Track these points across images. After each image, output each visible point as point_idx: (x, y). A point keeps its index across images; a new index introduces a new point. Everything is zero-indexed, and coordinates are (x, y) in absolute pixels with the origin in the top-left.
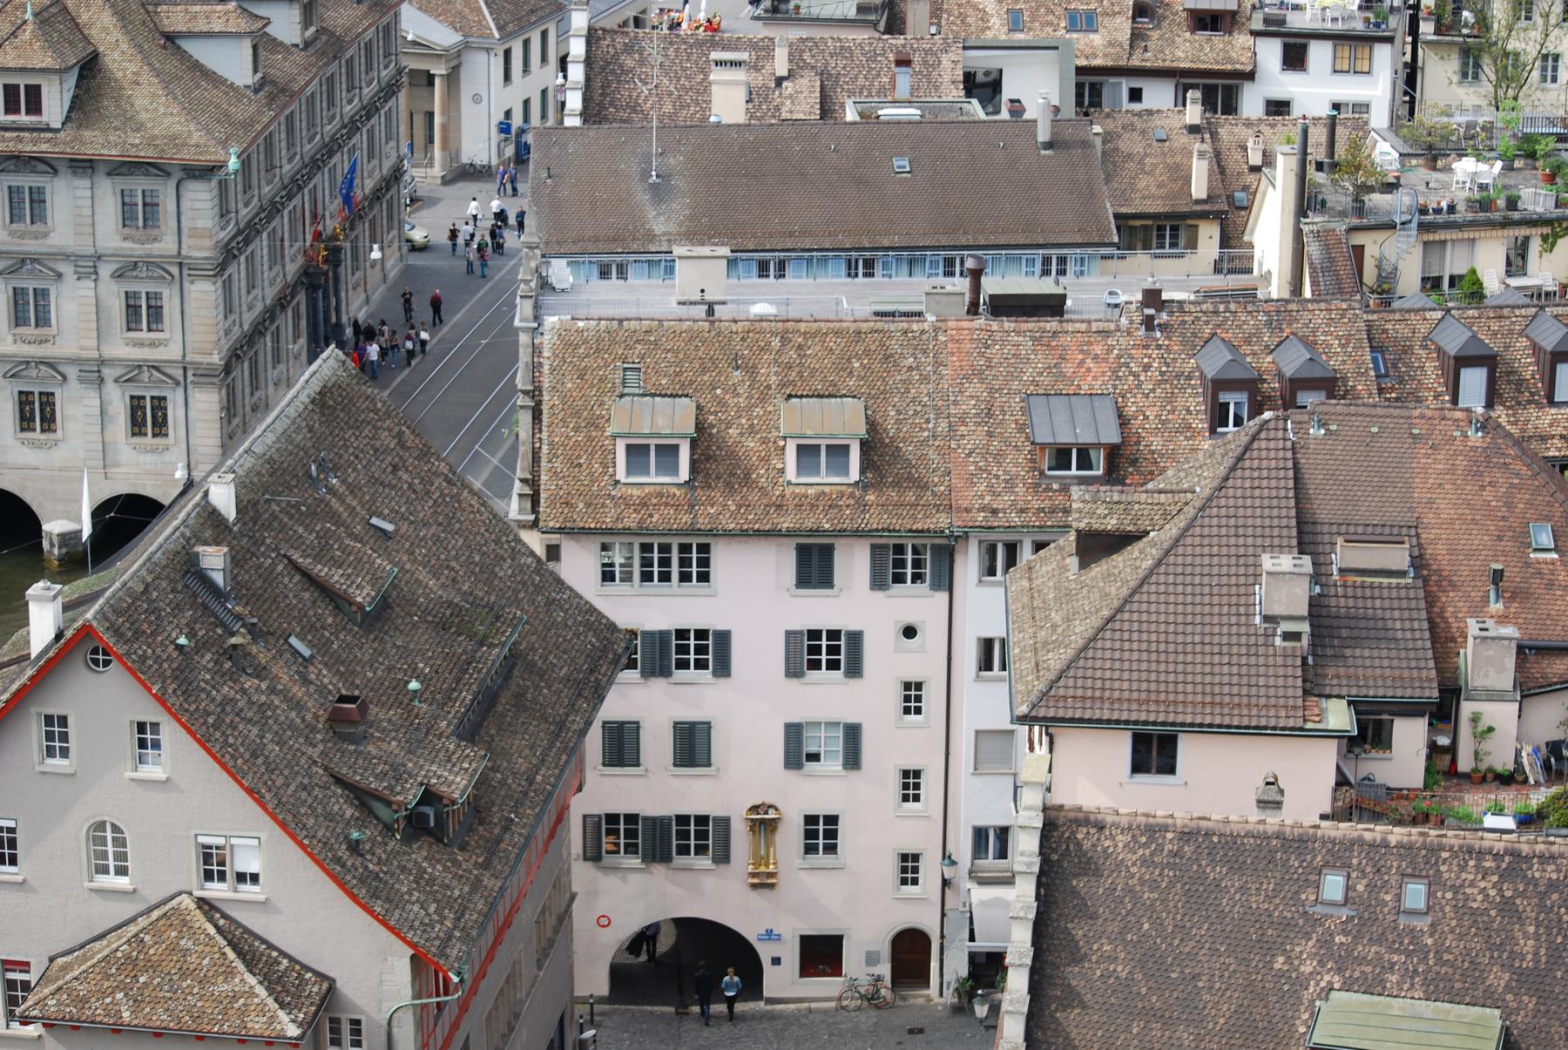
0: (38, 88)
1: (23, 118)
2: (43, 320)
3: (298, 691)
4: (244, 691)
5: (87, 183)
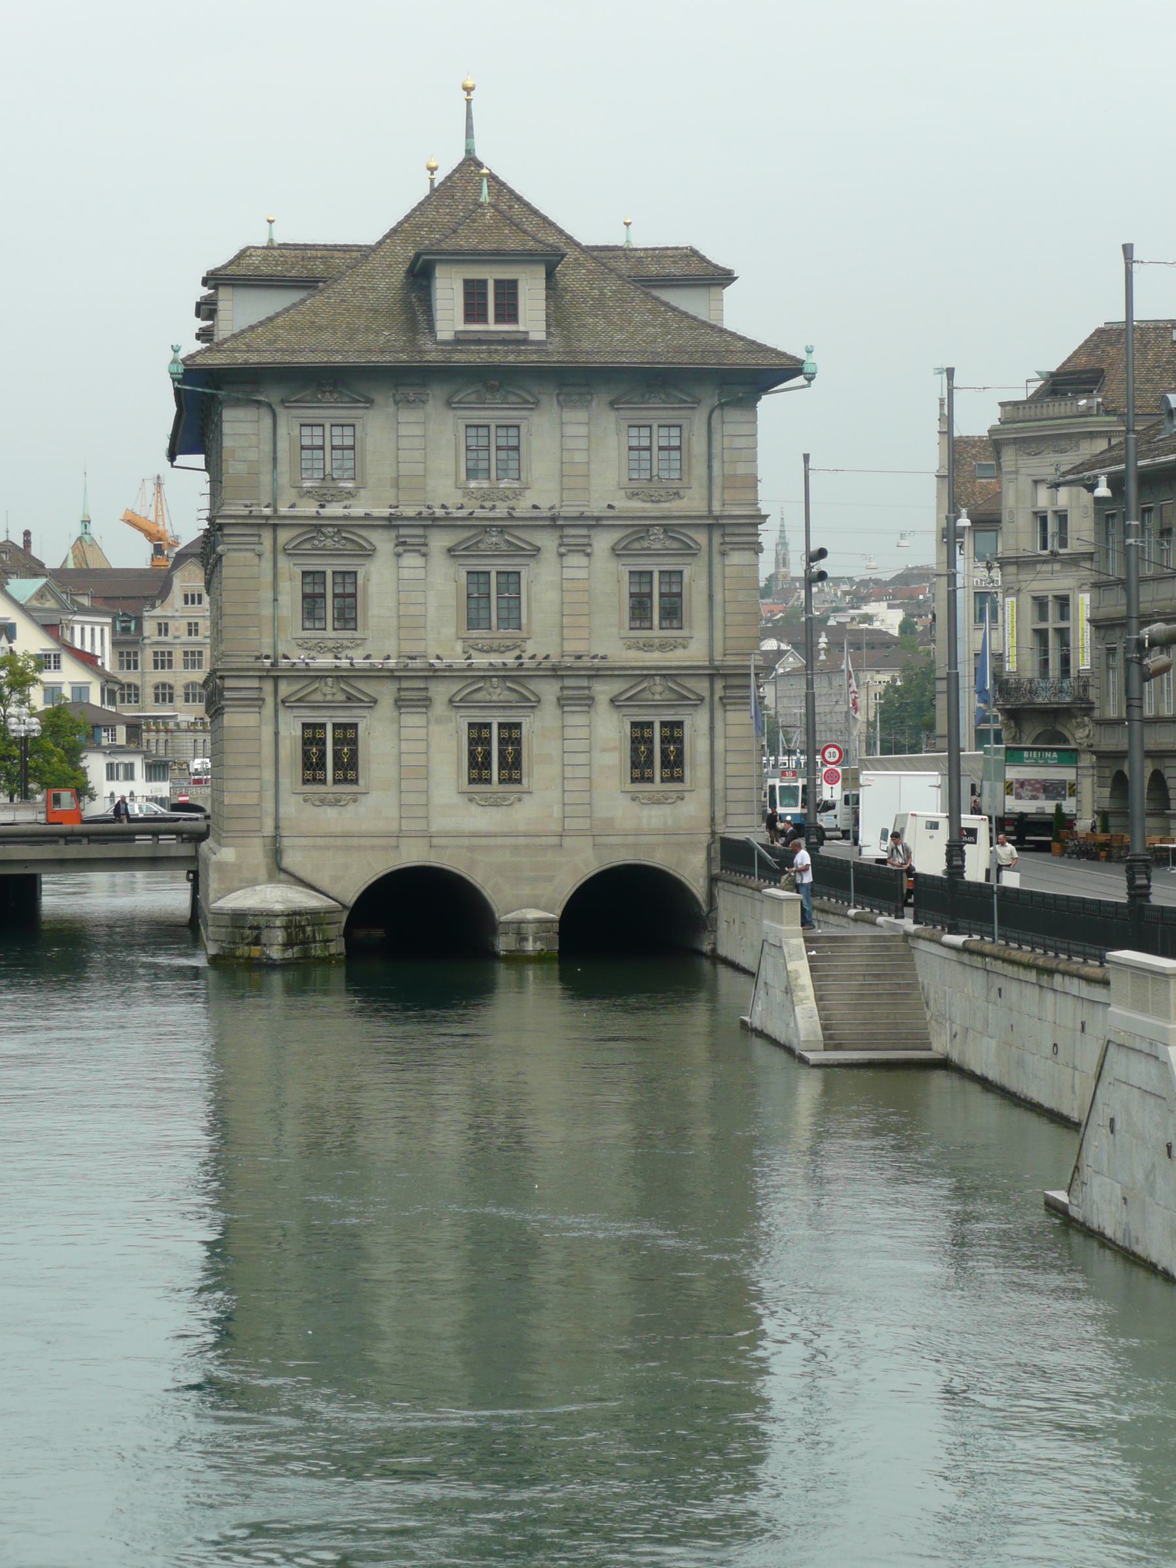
0: (513, 284)
5: (581, 415)
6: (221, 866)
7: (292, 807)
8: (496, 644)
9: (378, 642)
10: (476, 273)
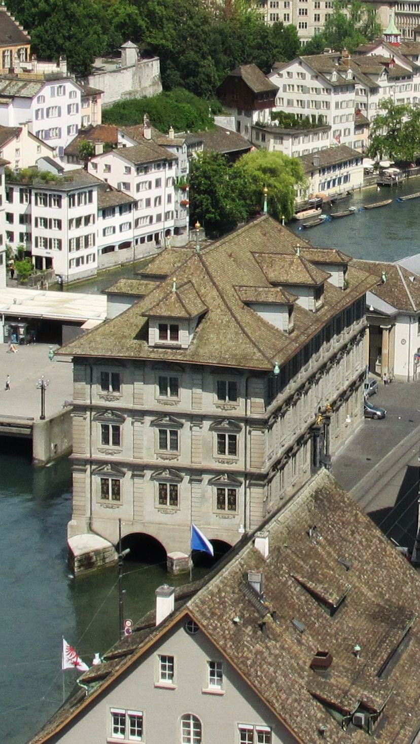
1: (169, 342)
2: (175, 446)
3: (296, 648)
4: (267, 648)
5: (199, 377)
6: (72, 527)
7: (96, 507)
8: (168, 456)
9: (124, 454)
10: (163, 322)
